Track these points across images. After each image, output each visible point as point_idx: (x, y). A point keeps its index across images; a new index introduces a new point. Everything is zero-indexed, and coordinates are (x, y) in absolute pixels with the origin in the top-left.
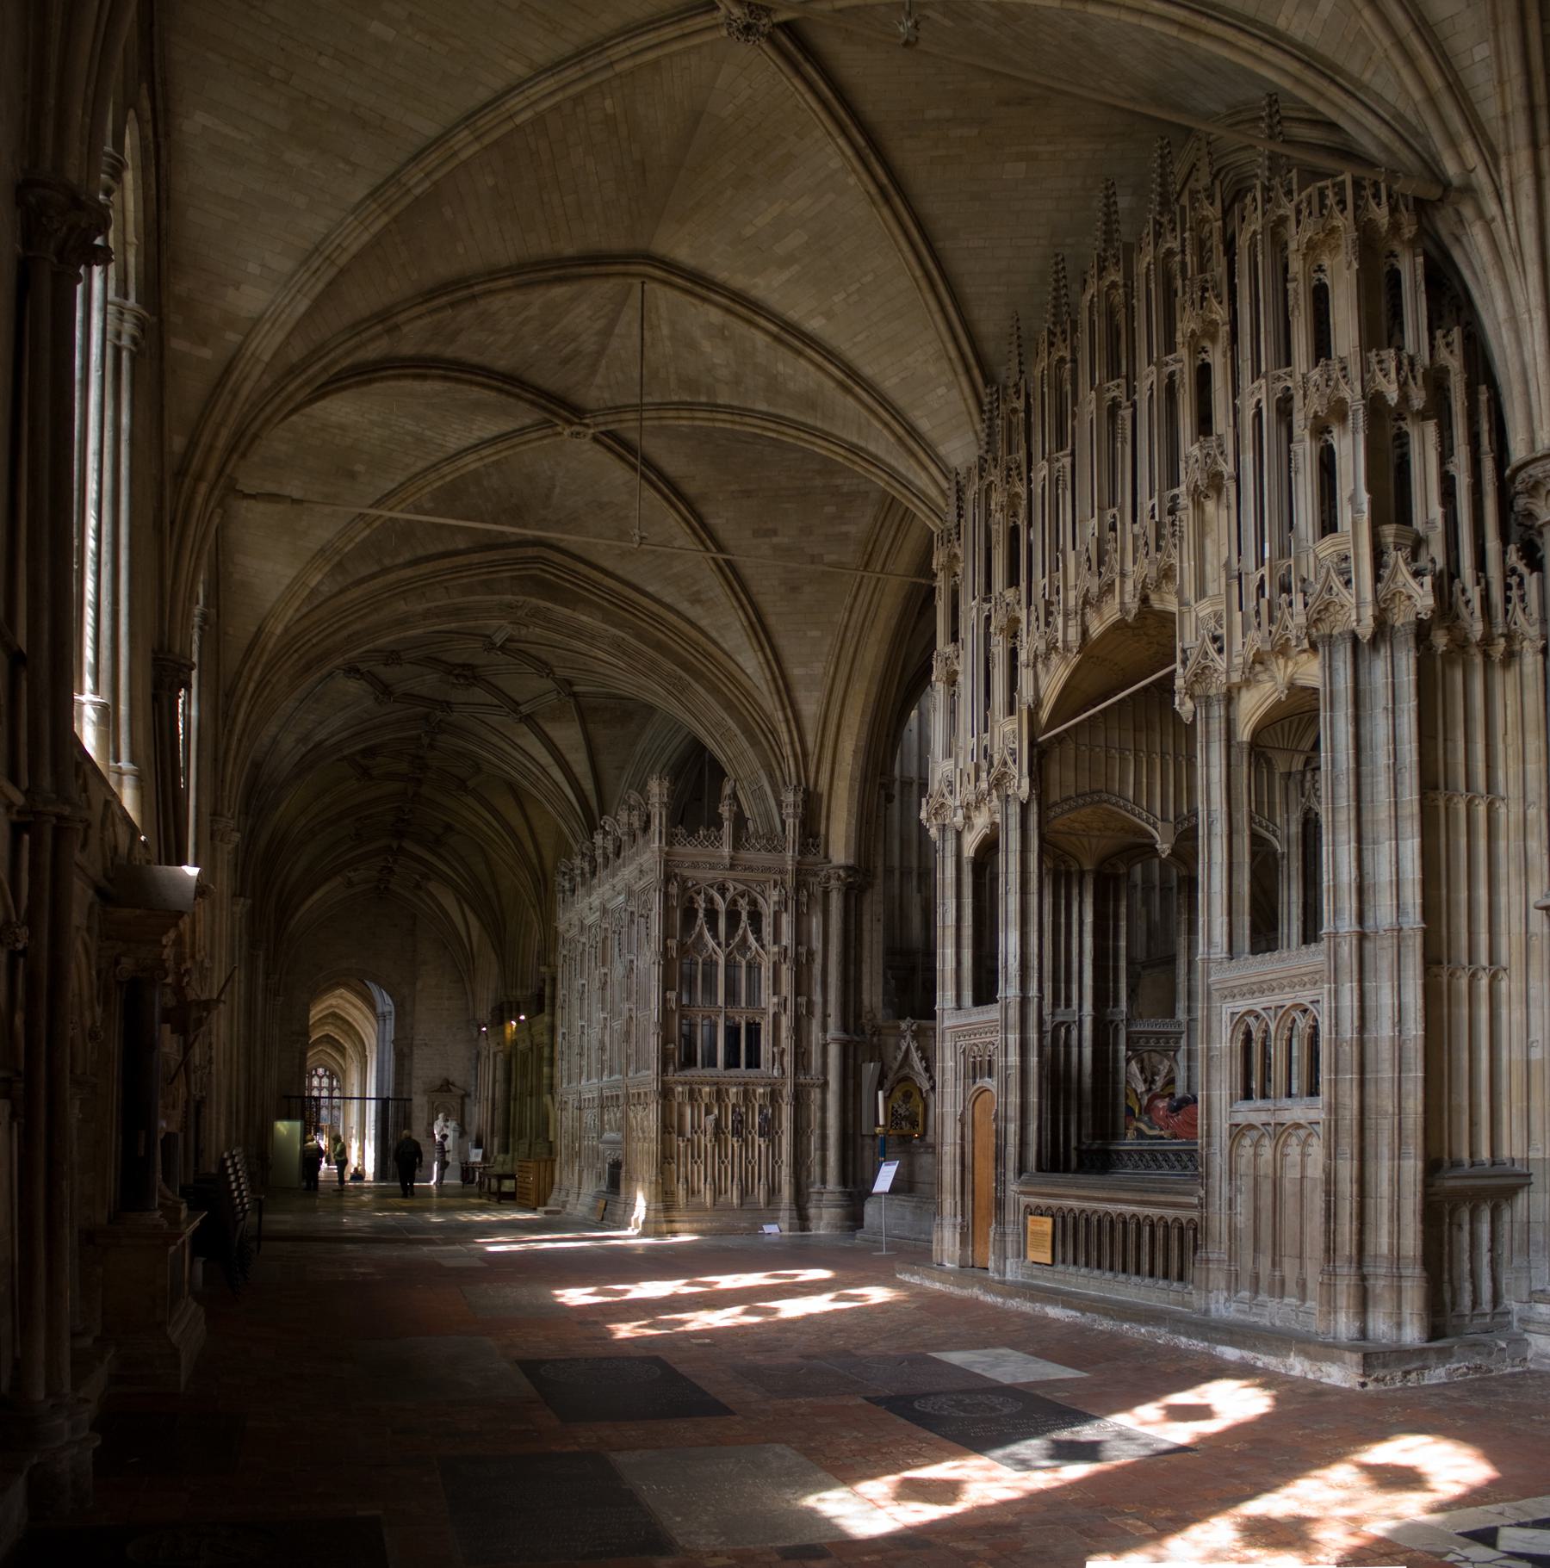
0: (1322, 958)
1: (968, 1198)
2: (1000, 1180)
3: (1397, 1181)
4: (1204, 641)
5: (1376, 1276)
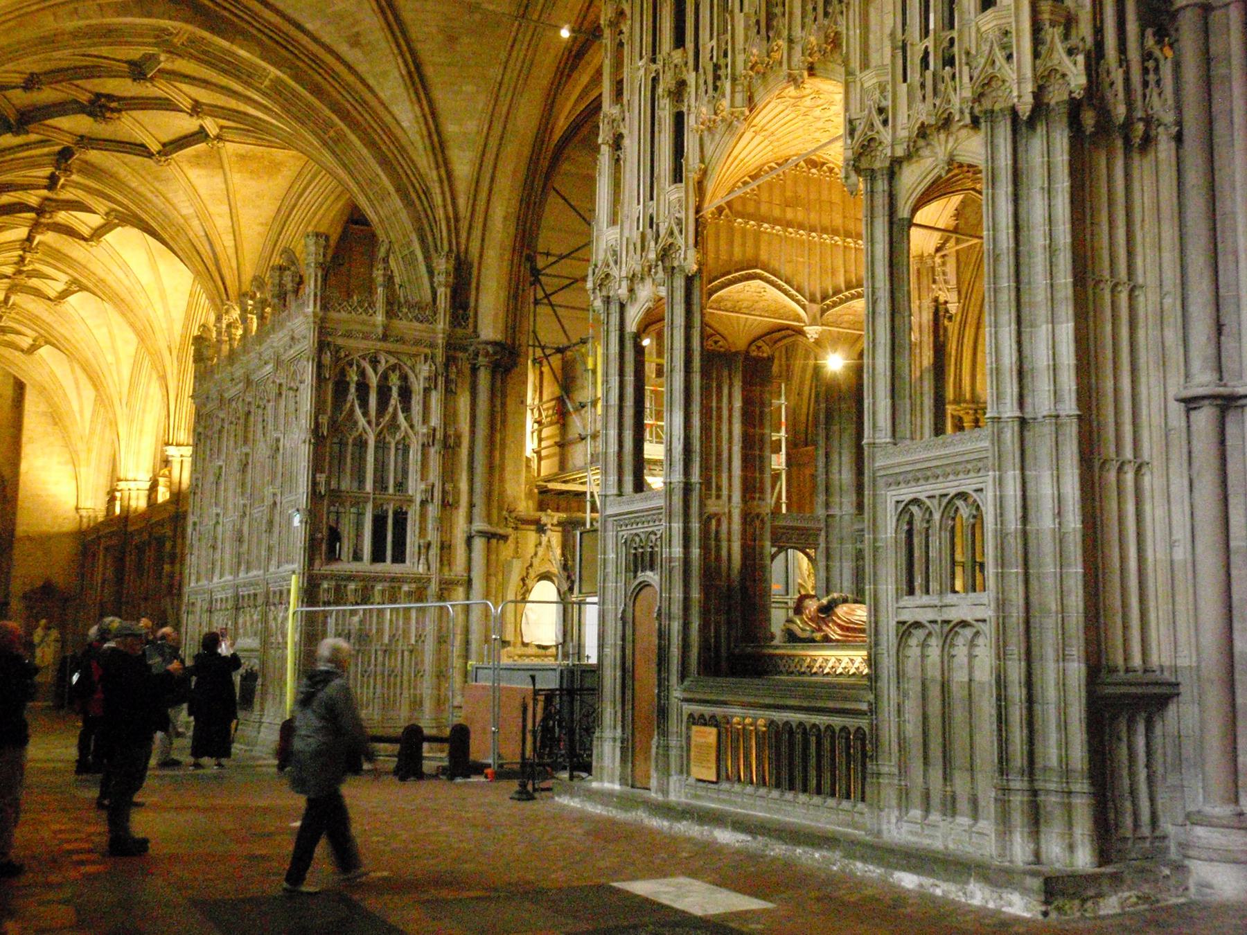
0: (986, 444)
1: (629, 706)
2: (662, 684)
3: (1062, 685)
4: (870, 112)
5: (1048, 792)
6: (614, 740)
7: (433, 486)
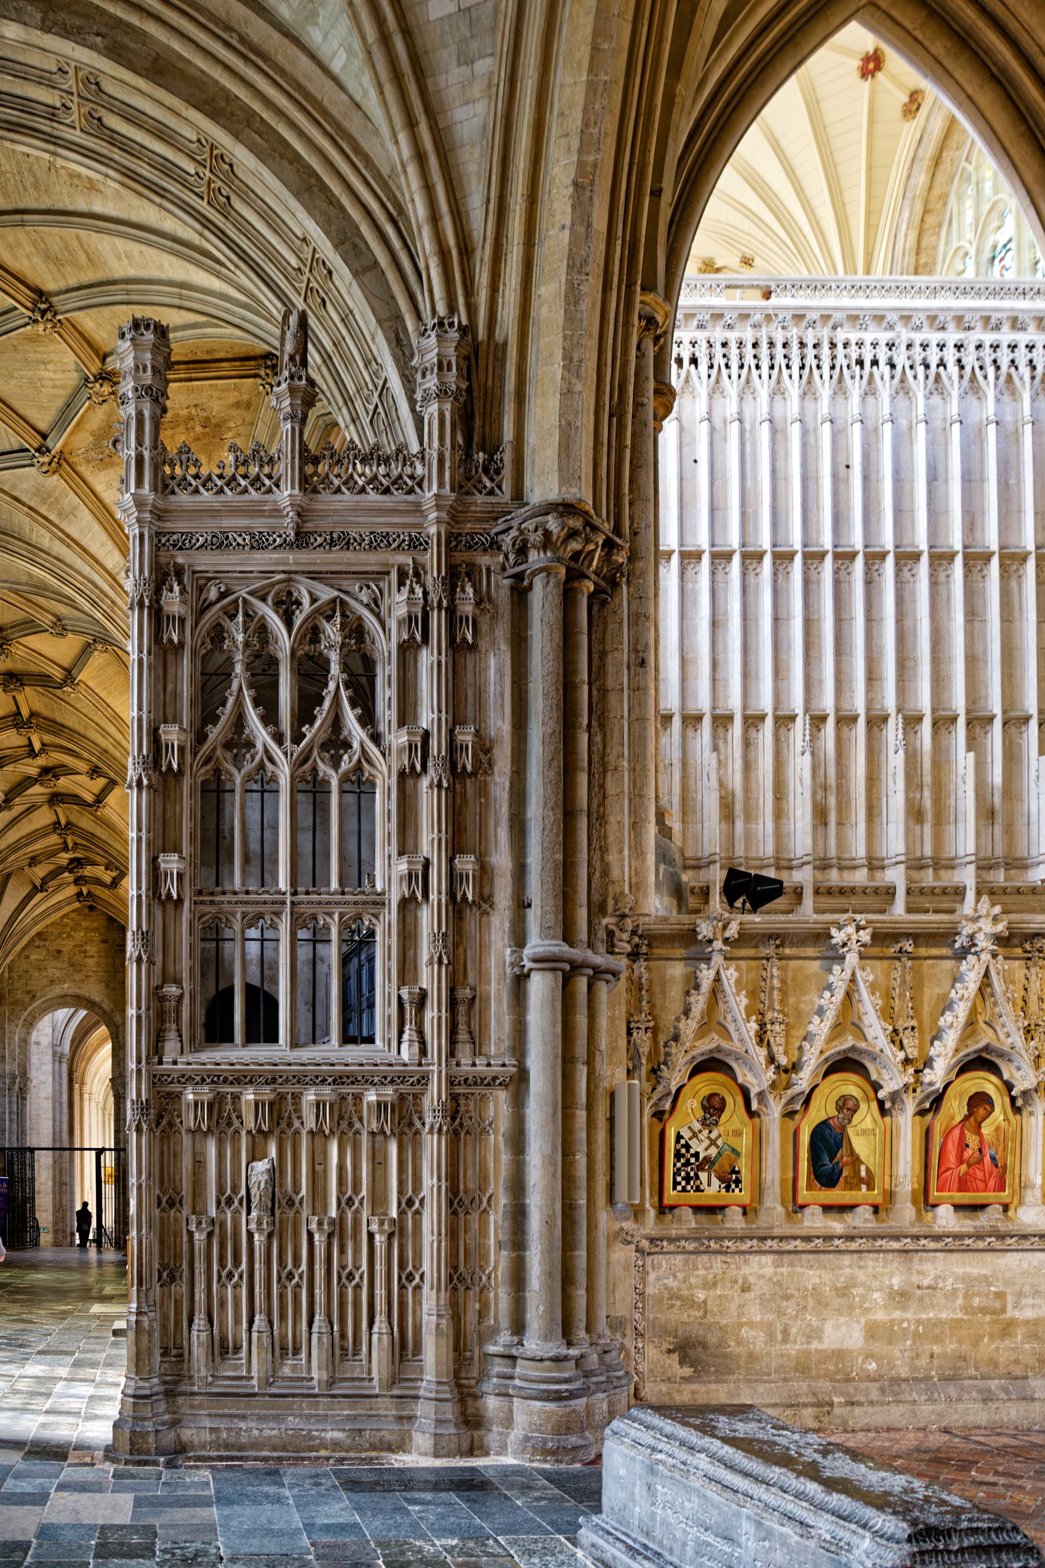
7: (427, 863)
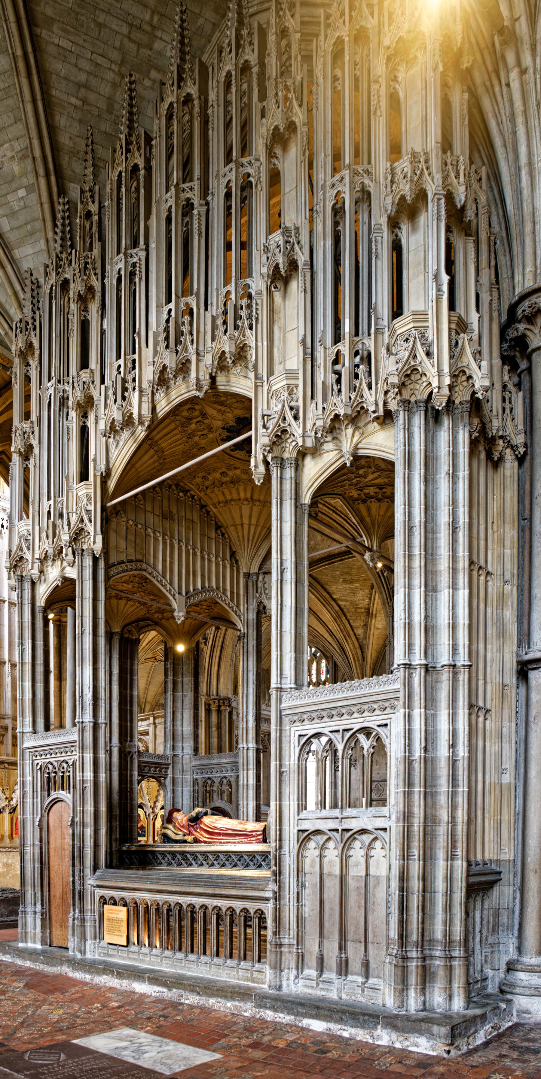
1: (46, 889)
6: (35, 913)
